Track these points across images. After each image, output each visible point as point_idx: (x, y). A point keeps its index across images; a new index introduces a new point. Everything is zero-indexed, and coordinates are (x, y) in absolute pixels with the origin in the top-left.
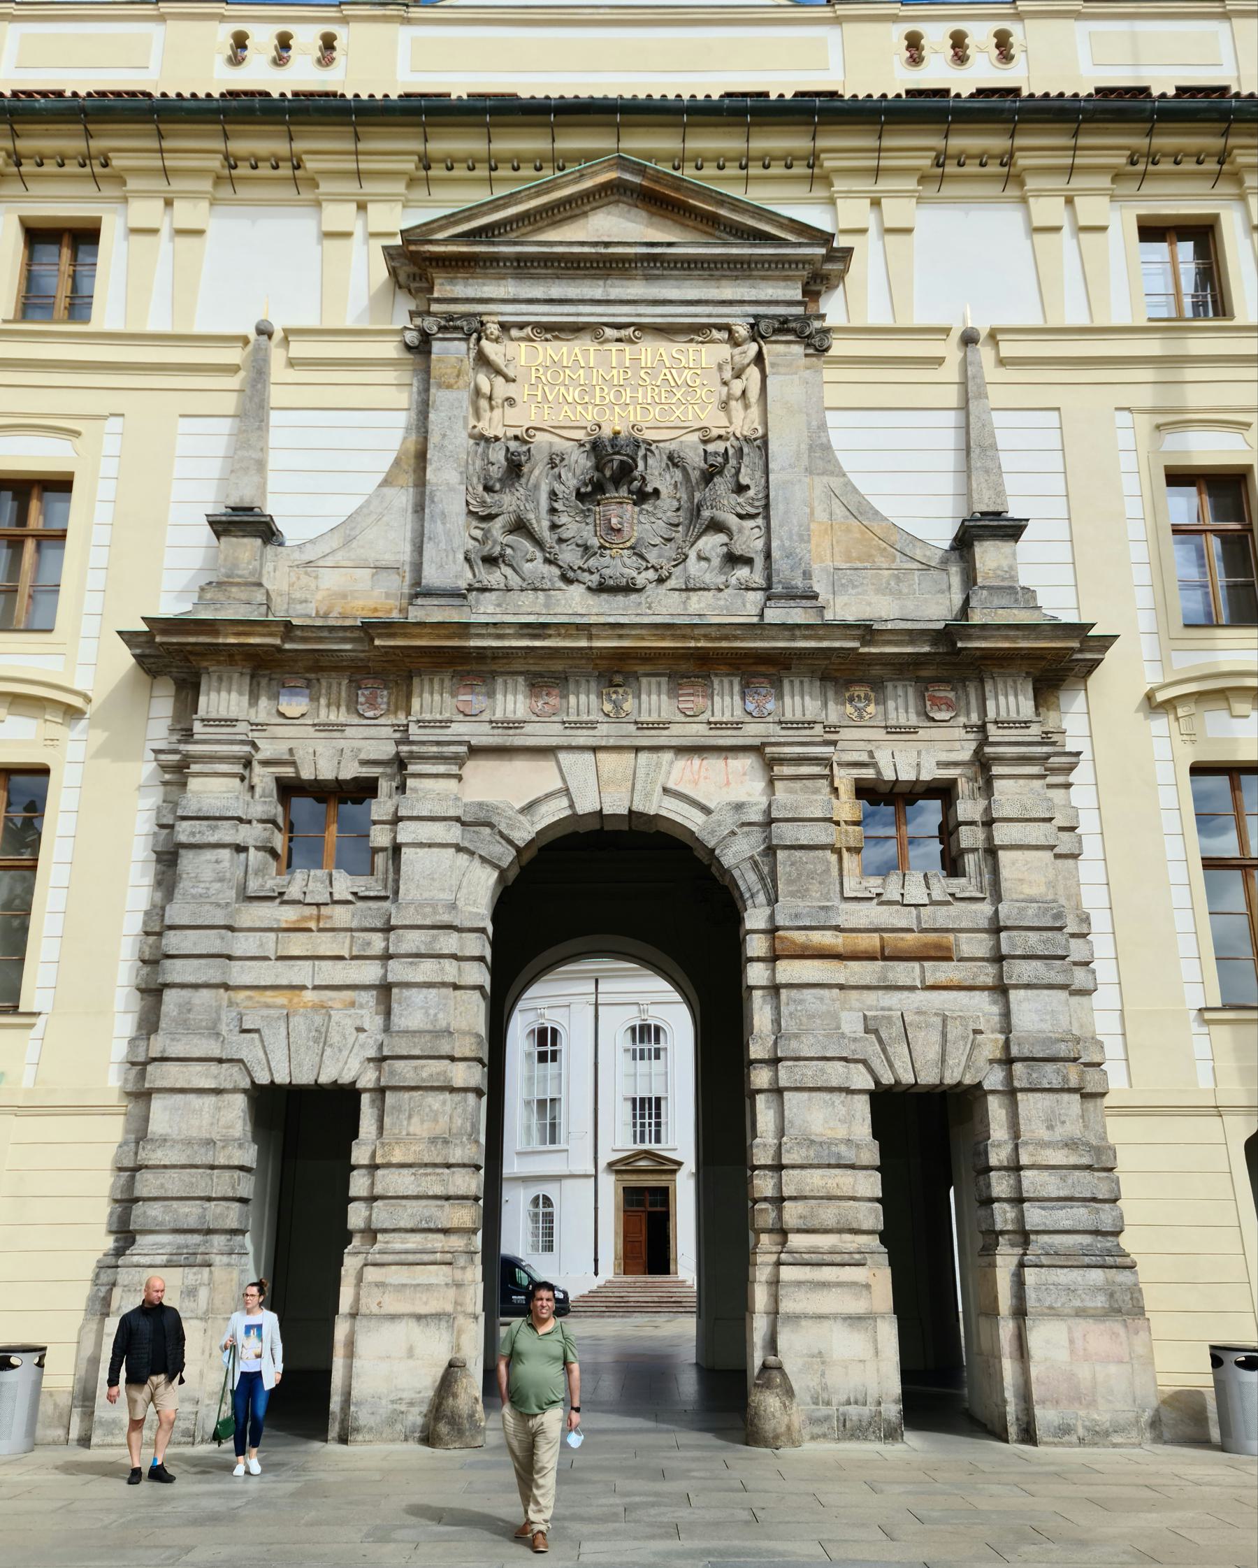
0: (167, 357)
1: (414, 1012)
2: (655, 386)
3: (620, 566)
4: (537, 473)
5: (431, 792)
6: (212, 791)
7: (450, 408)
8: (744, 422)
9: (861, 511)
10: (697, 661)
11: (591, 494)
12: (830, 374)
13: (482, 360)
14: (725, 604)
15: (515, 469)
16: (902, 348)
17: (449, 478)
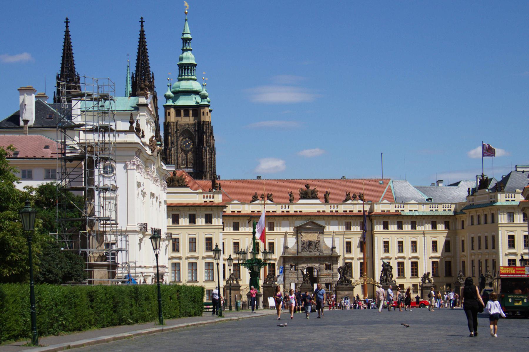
0: (279, 234)
1: (300, 279)
2: (312, 237)
3: (311, 250)
4: (305, 244)
5: (300, 266)
6: (287, 266)
7: (299, 238)
8: (319, 240)
9: (326, 245)
10: (316, 257)
11: (309, 245)
12: (325, 236)
13: (302, 235)
14: (318, 254)
15: (304, 244)
16: (329, 233)
17: (300, 244)
